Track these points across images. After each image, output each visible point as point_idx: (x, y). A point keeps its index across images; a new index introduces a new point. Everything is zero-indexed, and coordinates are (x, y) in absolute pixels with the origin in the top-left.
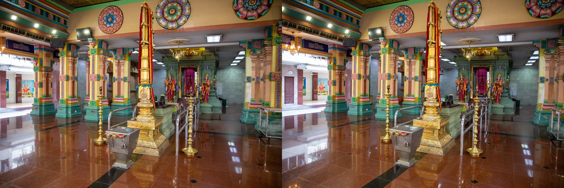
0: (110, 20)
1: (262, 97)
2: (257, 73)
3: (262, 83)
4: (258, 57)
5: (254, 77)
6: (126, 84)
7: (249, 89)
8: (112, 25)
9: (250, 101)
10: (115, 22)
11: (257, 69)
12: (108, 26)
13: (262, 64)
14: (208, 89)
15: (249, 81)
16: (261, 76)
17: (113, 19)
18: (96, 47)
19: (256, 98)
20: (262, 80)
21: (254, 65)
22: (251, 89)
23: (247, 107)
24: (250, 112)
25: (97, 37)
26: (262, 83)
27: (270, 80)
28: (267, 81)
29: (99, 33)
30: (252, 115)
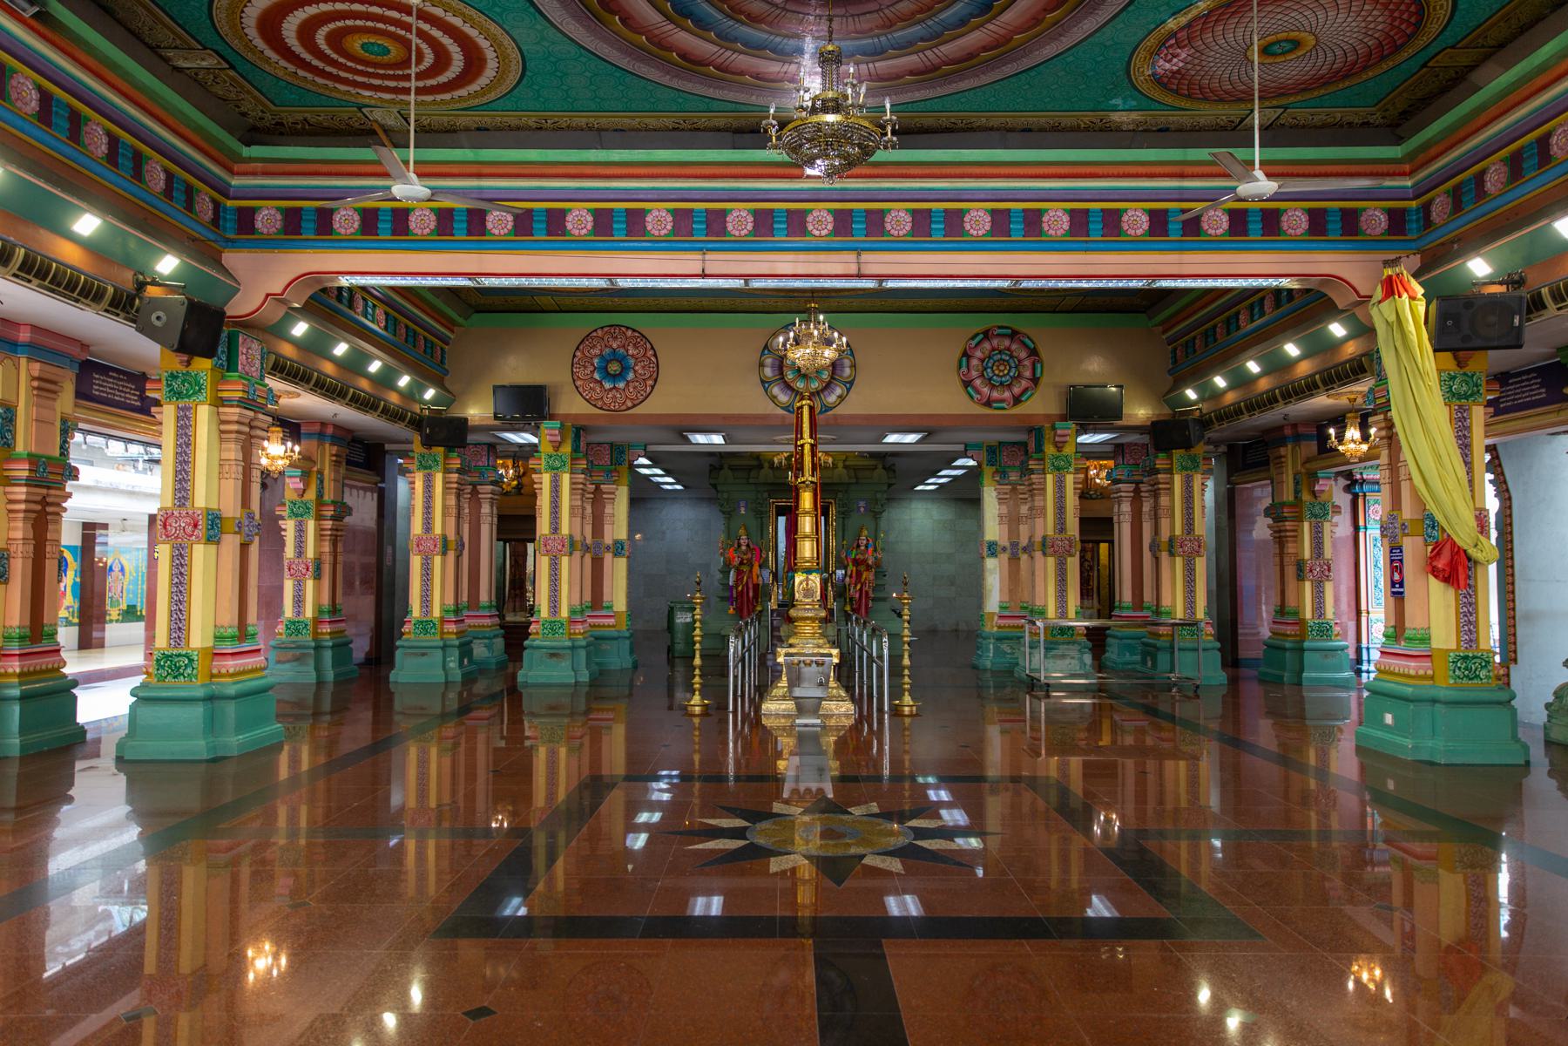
0: (614, 368)
1: (1026, 596)
2: (1013, 532)
3: (1024, 557)
4: (1014, 490)
5: (1005, 542)
6: (622, 563)
7: (994, 573)
8: (621, 385)
9: (997, 610)
10: (631, 376)
11: (1012, 521)
12: (608, 385)
13: (1024, 509)
14: (868, 576)
15: (993, 555)
16: (1024, 542)
17: (625, 369)
18: (567, 449)
19: (1011, 599)
20: (1025, 549)
21: (1005, 510)
22: (997, 576)
23: (991, 628)
24: (999, 639)
25: (567, 416)
26: (1024, 557)
27: (1045, 554)
28: (1038, 555)
29: (572, 404)
30: (1005, 647)
